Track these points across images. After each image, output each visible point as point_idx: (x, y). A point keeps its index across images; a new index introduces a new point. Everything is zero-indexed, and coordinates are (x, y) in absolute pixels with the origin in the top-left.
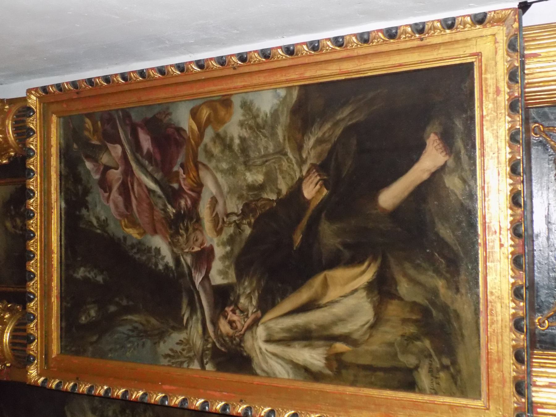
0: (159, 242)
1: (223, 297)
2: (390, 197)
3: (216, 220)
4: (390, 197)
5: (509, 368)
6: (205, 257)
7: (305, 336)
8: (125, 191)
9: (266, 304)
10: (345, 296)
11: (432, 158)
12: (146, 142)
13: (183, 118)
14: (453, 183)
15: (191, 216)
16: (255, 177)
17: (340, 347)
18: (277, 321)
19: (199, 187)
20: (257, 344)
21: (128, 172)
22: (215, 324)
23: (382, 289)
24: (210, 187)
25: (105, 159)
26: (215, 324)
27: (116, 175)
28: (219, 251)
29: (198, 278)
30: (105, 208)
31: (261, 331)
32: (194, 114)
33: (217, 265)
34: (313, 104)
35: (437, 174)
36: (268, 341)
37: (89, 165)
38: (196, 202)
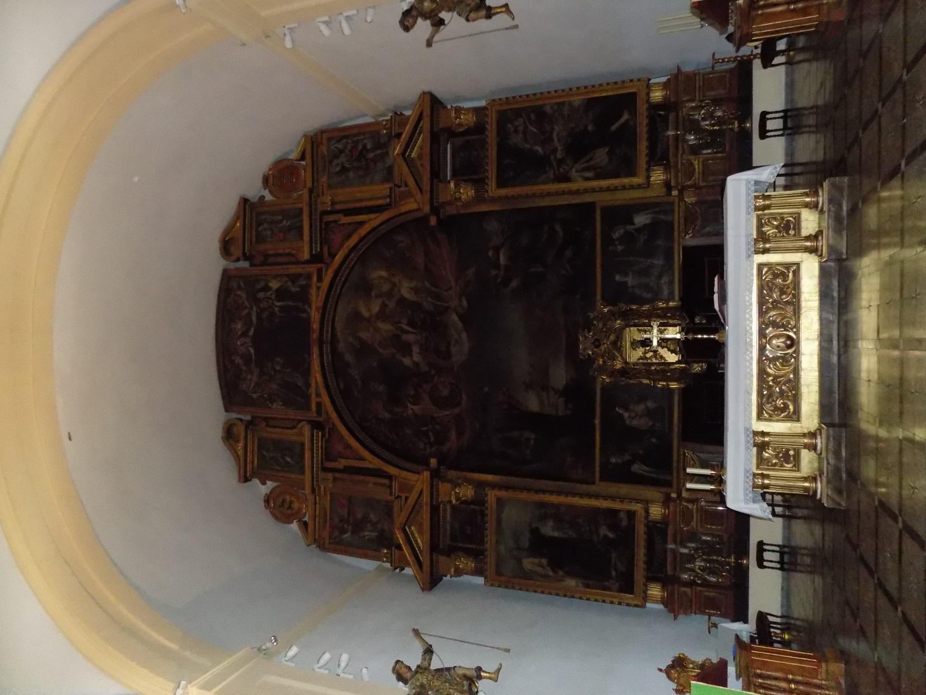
0: (539, 149)
1: (560, 162)
2: (614, 128)
3: (559, 140)
4: (614, 128)
5: (644, 166)
6: (555, 151)
7: (588, 169)
8: (524, 133)
9: (575, 163)
10: (601, 155)
11: (626, 117)
12: (533, 117)
13: (548, 109)
14: (631, 123)
15: (550, 139)
16: (572, 125)
17: (598, 170)
18: (579, 166)
19: (553, 129)
20: (573, 173)
21: (526, 127)
22: (558, 169)
23: (609, 154)
24: (556, 128)
25: (516, 123)
26: (558, 169)
27: (521, 128)
28: (559, 148)
29: (552, 157)
30: (516, 139)
31: (574, 170)
32: (552, 108)
33: (559, 152)
34: (591, 104)
35: (627, 121)
36: (577, 171)
37: (509, 126)
38: (552, 133)
